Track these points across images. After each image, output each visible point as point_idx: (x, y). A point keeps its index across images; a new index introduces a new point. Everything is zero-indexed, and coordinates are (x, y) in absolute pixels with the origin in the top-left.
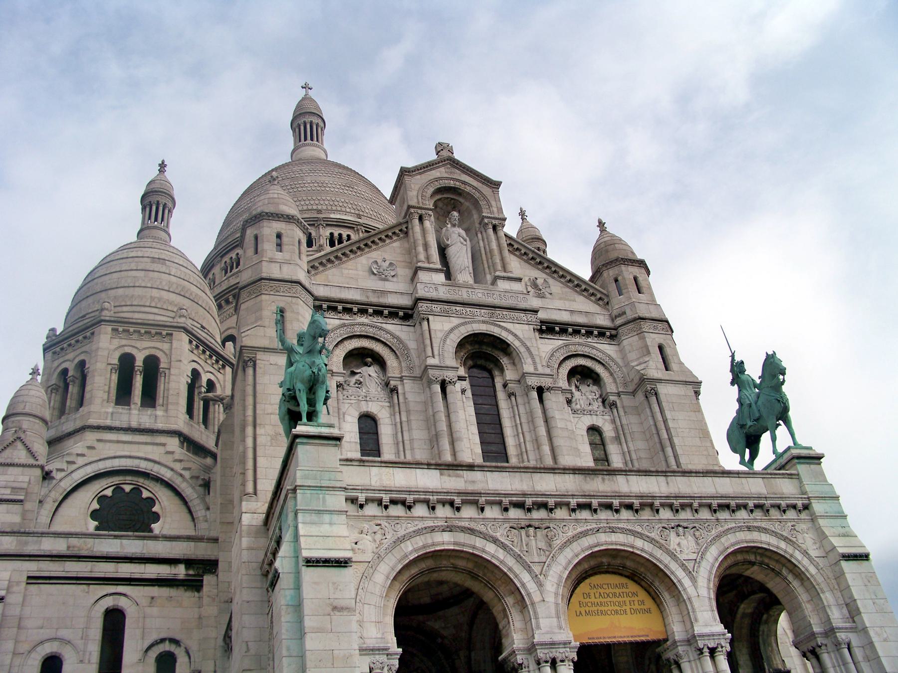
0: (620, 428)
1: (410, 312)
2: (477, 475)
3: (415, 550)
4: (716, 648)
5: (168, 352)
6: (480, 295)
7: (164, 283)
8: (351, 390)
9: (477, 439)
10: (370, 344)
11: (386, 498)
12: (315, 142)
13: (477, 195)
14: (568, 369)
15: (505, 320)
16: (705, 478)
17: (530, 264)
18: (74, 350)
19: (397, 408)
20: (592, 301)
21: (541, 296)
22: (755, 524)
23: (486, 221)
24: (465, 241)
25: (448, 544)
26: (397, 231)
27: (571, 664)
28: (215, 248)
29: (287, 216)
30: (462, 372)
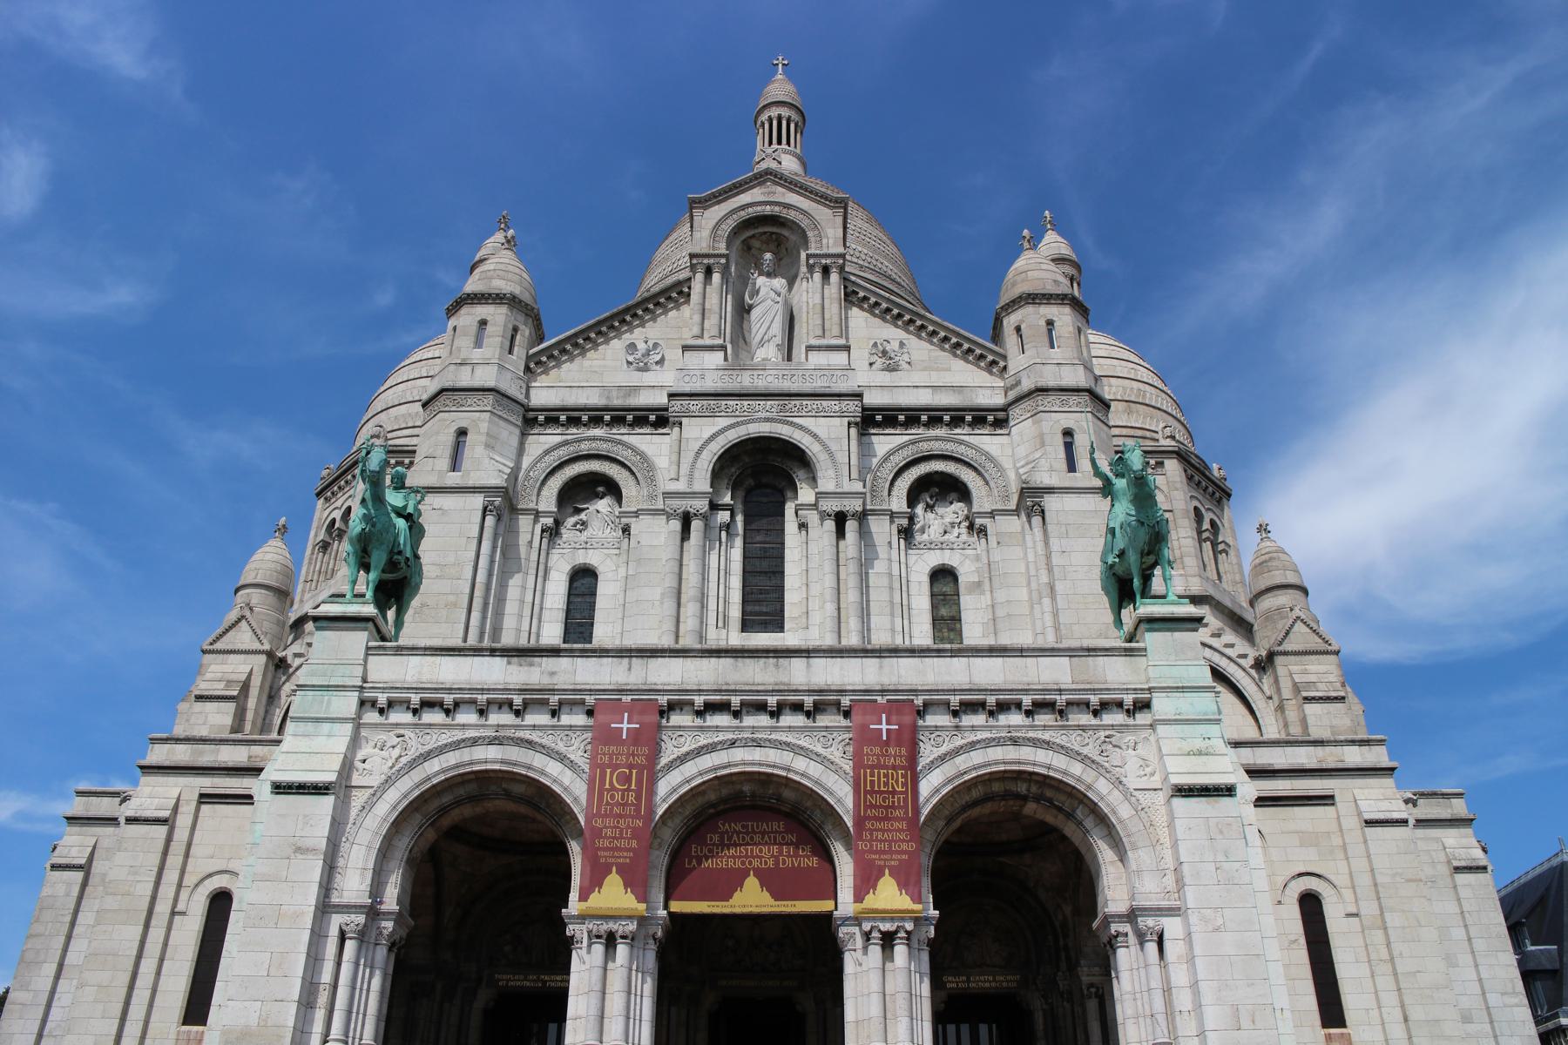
0: (986, 568)
2: (564, 663)
3: (443, 771)
4: (896, 932)
6: (770, 379)
8: (567, 534)
9: (736, 596)
10: (602, 467)
11: (415, 699)
12: (784, 146)
13: (804, 223)
14: (912, 480)
15: (804, 414)
16: (956, 659)
19: (625, 557)
21: (892, 368)
22: (1031, 734)
23: (811, 261)
24: (779, 295)
25: (494, 762)
27: (652, 941)
29: (497, 295)
30: (727, 499)
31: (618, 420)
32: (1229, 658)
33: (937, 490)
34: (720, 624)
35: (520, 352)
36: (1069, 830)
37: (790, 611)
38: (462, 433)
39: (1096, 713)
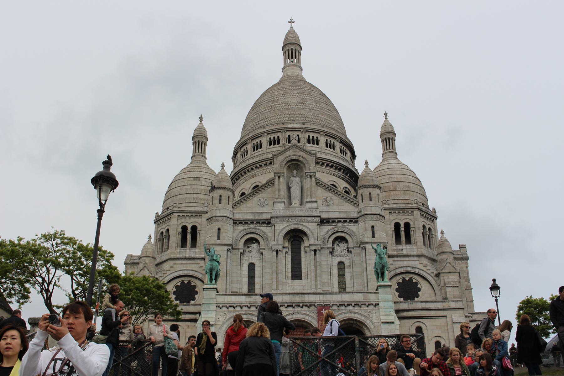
0: (351, 262)
1: (270, 221)
5: (200, 223)
6: (297, 212)
7: (199, 190)
9: (290, 271)
11: (228, 306)
17: (326, 190)
18: (165, 224)
20: (351, 204)
22: (354, 311)
26: (270, 184)
28: (241, 139)
30: (286, 245)
31: (258, 223)
32: (428, 274)
33: (340, 240)
34: (287, 278)
35: (231, 203)
36: (362, 330)
37: (303, 274)
38: (219, 229)
39: (367, 306)
